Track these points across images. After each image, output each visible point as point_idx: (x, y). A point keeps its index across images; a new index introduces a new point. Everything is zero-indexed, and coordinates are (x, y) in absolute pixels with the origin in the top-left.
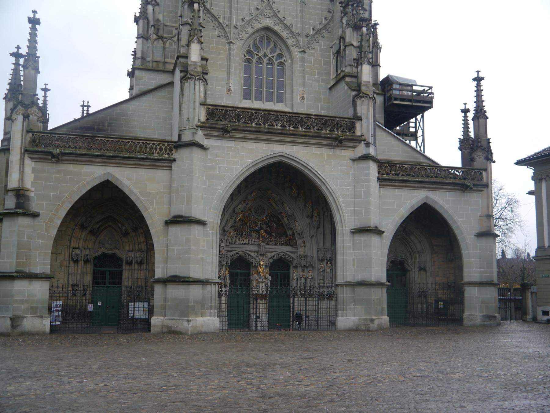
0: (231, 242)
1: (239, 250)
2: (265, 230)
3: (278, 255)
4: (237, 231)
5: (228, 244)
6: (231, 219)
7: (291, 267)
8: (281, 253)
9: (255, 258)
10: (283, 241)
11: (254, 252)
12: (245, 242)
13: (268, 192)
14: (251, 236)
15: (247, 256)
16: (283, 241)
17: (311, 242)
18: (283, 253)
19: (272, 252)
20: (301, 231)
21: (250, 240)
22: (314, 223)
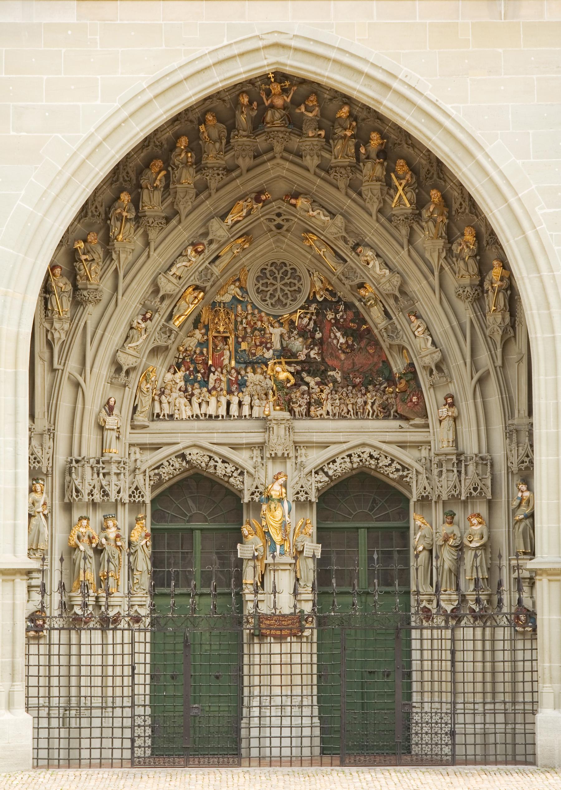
0: (157, 410)
1: (183, 442)
2: (302, 357)
3: (350, 456)
4: (188, 369)
5: (141, 419)
6: (145, 319)
7: (412, 503)
8: (359, 451)
9: (252, 471)
10: (370, 402)
11: (250, 446)
12: (211, 410)
13: (294, 206)
14: (242, 384)
15: (220, 464)
16: (370, 402)
17: (479, 400)
18: (368, 450)
19: (325, 445)
20: (437, 356)
21: (235, 400)
22: (490, 319)
